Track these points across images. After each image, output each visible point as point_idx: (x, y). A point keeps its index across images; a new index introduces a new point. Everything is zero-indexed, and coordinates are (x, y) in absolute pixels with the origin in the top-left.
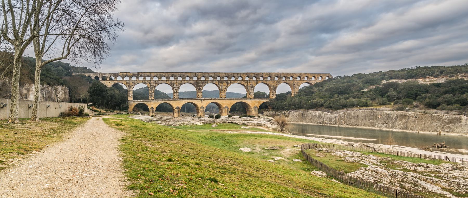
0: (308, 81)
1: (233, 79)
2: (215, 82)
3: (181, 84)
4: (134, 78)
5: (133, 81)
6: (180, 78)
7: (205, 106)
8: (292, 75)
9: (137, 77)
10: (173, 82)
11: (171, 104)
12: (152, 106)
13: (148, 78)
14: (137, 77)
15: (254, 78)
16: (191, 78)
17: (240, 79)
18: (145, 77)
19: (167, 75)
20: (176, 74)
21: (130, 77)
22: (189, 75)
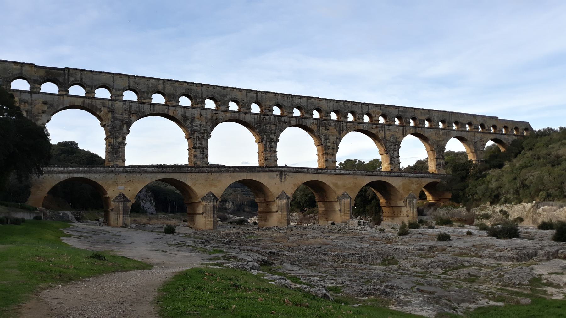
0: (498, 137)
1: (350, 118)
2: (309, 123)
3: (215, 123)
4: (50, 88)
5: (48, 98)
6: (210, 104)
7: (290, 192)
8: (469, 120)
9: (64, 86)
10: (189, 113)
11: (189, 183)
12: (122, 189)
13: (102, 93)
14: (64, 86)
15: (397, 122)
16: (244, 106)
17: (366, 119)
18: (90, 89)
19: (169, 89)
20: (199, 89)
21: (36, 83)
22: (239, 96)
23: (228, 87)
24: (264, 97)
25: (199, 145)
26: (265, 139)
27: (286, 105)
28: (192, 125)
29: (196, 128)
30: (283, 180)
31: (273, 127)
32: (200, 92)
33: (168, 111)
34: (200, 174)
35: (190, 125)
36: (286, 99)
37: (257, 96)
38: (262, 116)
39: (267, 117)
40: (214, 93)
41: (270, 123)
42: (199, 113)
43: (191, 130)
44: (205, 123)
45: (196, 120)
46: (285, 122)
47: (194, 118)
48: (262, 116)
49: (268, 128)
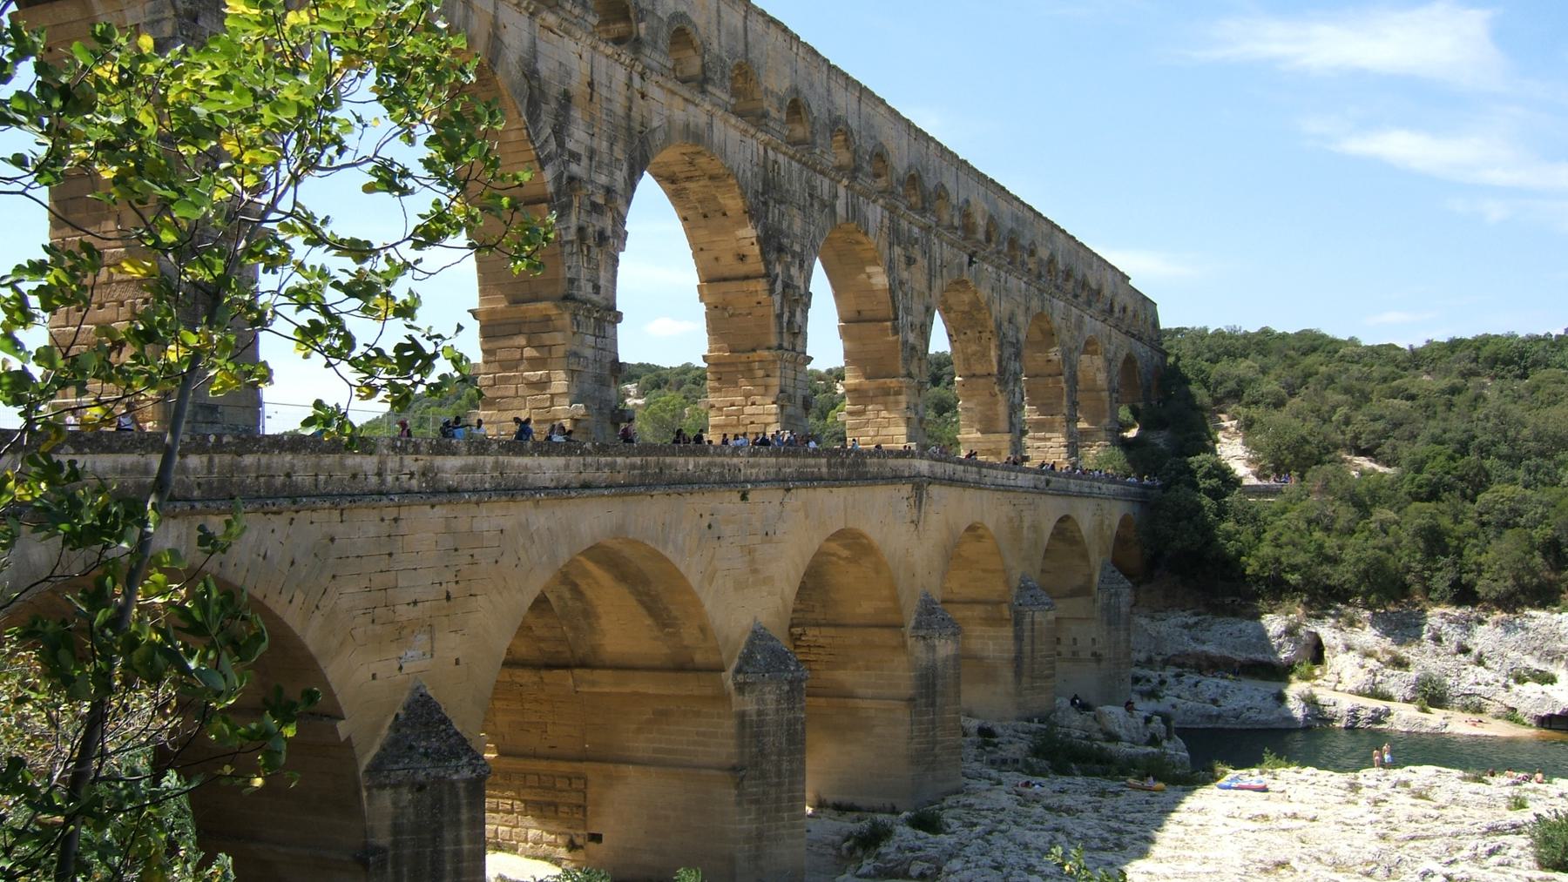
11: (691, 568)
25: (586, 290)
26: (779, 287)
28: (561, 144)
33: (466, 17)
35: (553, 146)
38: (770, 153)
39: (781, 158)
43: (558, 178)
44: (605, 144)
45: (576, 114)
47: (566, 99)
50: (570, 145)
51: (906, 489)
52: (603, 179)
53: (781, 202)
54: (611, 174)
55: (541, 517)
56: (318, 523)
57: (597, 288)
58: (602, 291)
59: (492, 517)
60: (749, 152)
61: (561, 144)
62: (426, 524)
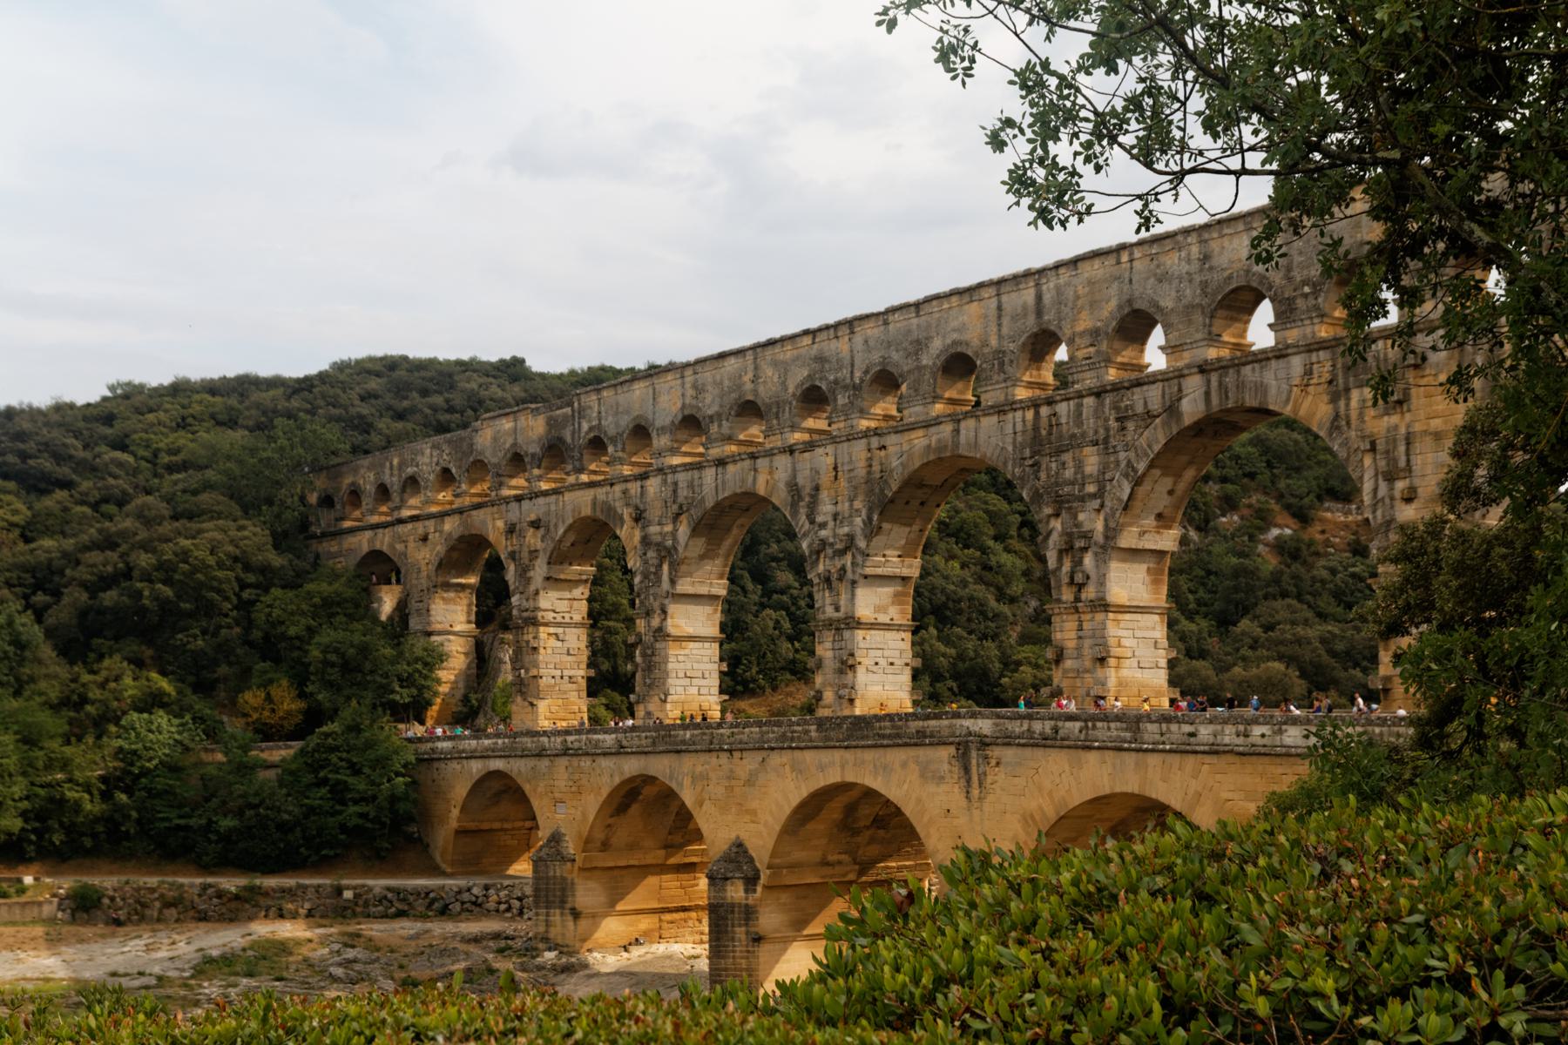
23: (928, 300)
24: (1070, 293)
27: (1167, 303)
29: (823, 533)
30: (975, 792)
31: (1092, 461)
32: (847, 361)
34: (713, 759)
35: (807, 526)
36: (1172, 261)
37: (1039, 297)
40: (889, 344)
41: (1074, 443)
42: (830, 460)
45: (824, 495)
46: (1149, 416)
47: (817, 488)
48: (1044, 411)
49: (1069, 473)
50: (819, 519)
51: (945, 753)
52: (846, 530)
53: (1059, 451)
54: (851, 524)
55: (606, 763)
56: (531, 762)
57: (837, 609)
58: (842, 609)
59: (586, 763)
60: (1009, 429)
61: (812, 522)
62: (564, 761)
